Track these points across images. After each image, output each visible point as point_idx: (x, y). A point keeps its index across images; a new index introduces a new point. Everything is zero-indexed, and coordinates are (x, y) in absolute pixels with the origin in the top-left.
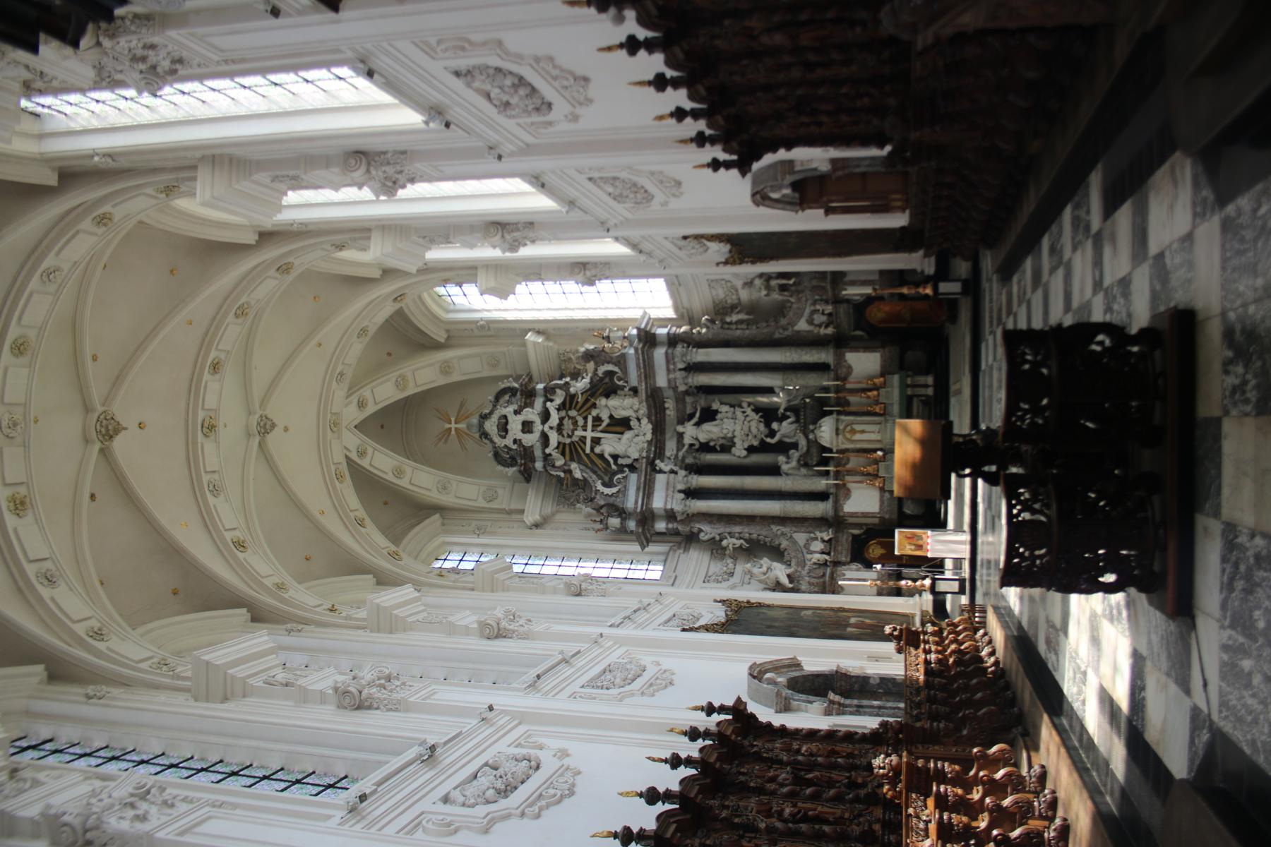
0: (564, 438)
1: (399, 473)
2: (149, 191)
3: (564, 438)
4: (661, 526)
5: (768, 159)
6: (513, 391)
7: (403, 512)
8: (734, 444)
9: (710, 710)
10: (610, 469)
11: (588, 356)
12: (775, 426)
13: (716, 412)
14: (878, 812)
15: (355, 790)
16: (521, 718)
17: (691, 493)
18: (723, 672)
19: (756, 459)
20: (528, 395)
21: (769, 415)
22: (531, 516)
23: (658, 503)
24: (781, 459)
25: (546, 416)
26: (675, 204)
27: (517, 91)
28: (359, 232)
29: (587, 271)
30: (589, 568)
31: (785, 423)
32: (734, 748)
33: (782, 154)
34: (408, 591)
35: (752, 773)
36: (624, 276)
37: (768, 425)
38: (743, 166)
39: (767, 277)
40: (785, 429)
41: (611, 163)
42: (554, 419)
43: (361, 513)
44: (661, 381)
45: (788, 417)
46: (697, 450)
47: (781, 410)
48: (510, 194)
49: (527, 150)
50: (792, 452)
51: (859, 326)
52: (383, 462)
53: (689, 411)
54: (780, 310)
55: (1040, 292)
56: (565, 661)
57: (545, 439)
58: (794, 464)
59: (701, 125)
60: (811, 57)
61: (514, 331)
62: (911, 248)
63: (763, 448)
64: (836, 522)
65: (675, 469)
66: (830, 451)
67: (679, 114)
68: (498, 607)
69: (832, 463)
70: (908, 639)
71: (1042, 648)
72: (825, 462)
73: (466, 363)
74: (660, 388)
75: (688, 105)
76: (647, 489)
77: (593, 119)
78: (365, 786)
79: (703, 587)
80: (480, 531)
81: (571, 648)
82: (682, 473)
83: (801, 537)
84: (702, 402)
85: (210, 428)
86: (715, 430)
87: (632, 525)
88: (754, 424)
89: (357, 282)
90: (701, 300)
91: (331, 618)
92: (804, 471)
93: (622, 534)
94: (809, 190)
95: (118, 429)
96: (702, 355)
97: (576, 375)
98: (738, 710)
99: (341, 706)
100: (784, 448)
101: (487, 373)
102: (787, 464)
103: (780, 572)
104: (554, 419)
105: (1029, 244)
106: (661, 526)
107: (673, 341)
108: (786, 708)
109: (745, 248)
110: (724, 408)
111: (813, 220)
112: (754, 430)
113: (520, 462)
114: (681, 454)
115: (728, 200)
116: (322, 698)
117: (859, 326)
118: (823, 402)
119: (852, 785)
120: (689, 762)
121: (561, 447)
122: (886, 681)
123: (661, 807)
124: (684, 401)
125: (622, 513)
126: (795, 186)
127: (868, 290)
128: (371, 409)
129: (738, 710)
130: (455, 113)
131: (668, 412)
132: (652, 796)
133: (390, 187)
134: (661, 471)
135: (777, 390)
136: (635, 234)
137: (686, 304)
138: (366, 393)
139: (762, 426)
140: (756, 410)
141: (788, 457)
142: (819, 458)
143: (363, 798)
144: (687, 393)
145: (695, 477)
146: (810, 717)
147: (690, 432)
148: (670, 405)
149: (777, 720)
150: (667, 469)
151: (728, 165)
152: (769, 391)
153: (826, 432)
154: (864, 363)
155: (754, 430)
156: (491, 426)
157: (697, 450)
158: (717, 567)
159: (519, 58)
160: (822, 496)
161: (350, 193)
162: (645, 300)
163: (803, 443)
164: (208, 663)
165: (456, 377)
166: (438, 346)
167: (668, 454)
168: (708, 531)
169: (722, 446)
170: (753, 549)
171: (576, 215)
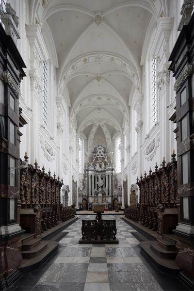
0: (99, 159)
1: (93, 132)
2: (163, 9)
3: (99, 159)
4: (87, 172)
5: (138, 187)
6: (105, 150)
7: (86, 133)
9: (62, 180)
10: (94, 165)
11: (110, 161)
14: (50, 204)
15: (45, 126)
16: (58, 153)
17: (91, 176)
18: (67, 182)
19: (96, 186)
20: (104, 153)
21: (102, 187)
22: (87, 154)
23: (90, 172)
25: (102, 155)
26: (132, 174)
27: (151, 150)
28: (130, 125)
29: (122, 160)
30: (80, 162)
32: (58, 184)
33: (139, 189)
34: (75, 134)
35: (54, 186)
36: (122, 166)
38: (137, 183)
39: (121, 186)
40: (100, 189)
41: (138, 165)
42: (101, 156)
43: (87, 126)
44: (107, 172)
48: (134, 148)
49: (141, 151)
51: (114, 199)
52: (94, 129)
54: (116, 188)
55: (122, 226)
56: (67, 159)
57: (98, 155)
59: (144, 177)
60: (153, 193)
61: (114, 150)
62: (125, 206)
63: (98, 186)
64: (88, 197)
67: (145, 174)
68: (74, 148)
70: (73, 206)
71: (73, 224)
73: (109, 142)
75: (147, 175)
76: (92, 170)
77: (145, 161)
78: (46, 128)
79: (79, 179)
80: (85, 146)
81: (69, 160)
83: (86, 192)
84: (104, 178)
85: (99, 98)
87: (87, 168)
89: (122, 124)
90: (118, 177)
91: (71, 121)
93: (85, 167)
94: (133, 192)
95: (99, 81)
96: (110, 178)
97: (107, 159)
98: (62, 184)
99: (58, 123)
100: (98, 189)
101: (108, 146)
102: (96, 190)
103: (81, 189)
104: (101, 156)
105: (126, 221)
106: (87, 172)
107: (112, 173)
108: (63, 191)
109: (125, 183)
111: (129, 193)
113: (95, 152)
115: (133, 181)
116: (58, 120)
117: (114, 199)
118: (104, 194)
119: (53, 200)
120: (55, 178)
121: (97, 158)
122: (67, 203)
123: (48, 174)
125: (88, 167)
126: (134, 190)
127: (119, 201)
128: (102, 127)
129: (62, 184)
130: (148, 140)
132: (49, 173)
133: (127, 150)
136: (128, 168)
137: (118, 175)
138: (105, 127)
142: (97, 194)
143: (44, 128)
146: (62, 194)
147: (100, 176)
148: (103, 173)
149: (61, 189)
151: (137, 181)
152: (105, 187)
153: (100, 195)
154: (109, 200)
156: (100, 147)
158: (81, 180)
159: (156, 150)
160: (91, 194)
161: (136, 122)
162: (118, 169)
164: (36, 30)
165: (107, 141)
166: (112, 138)
168: (86, 179)
170: (84, 185)
171: (131, 159)
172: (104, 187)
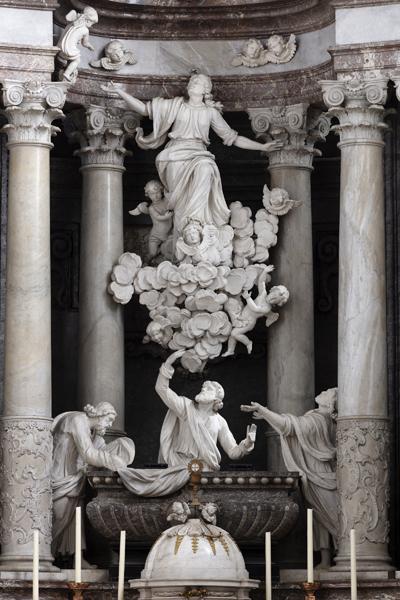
8: (151, 261)
12: (213, 392)
13: (255, 204)
21: (243, 373)
24: (108, 412)
31: (219, 423)
37: (215, 369)
40: (201, 429)
45: (239, 436)
46: (130, 143)
47: (263, 412)
50: (129, 446)
53: (259, 115)
58: (93, 452)
63: (142, 355)
65: (70, 73)
66: (134, 572)
69: (94, 575)
72: (99, 551)
74: (333, 20)
82: (58, 97)
86: (200, 193)
88: (217, 324)
92: (70, 484)
100: (142, 420)
102: (96, 434)
110: (267, 231)
112: (196, 325)
114: (118, 89)
118: (290, 550)
124: (291, 98)
131: (253, 46)
134: (60, 25)
135: (325, 398)
139: (209, 350)
140: (261, 332)
141: (111, 435)
144: (316, 107)
145: (45, 138)
147: (192, 118)
150: (70, 45)
152: (324, 372)
153: (195, 553)
155: (196, 325)
157: (130, 143)
163: (159, 481)
167: (119, 47)
169: (145, 222)
172: (289, 362)
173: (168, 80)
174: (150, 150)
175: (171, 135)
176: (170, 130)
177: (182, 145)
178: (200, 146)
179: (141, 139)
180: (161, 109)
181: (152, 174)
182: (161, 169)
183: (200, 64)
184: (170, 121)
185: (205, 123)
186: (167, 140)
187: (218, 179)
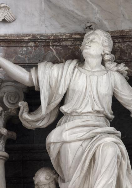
157: (13, 123)
173: (57, 40)
174: (38, 129)
175: (64, 109)
176: (62, 103)
177: (78, 121)
178: (101, 121)
179: (26, 117)
180: (50, 77)
181: (42, 159)
182: (53, 152)
183: (96, 16)
184: (62, 91)
185: (105, 90)
186: (59, 116)
187: (126, 162)
